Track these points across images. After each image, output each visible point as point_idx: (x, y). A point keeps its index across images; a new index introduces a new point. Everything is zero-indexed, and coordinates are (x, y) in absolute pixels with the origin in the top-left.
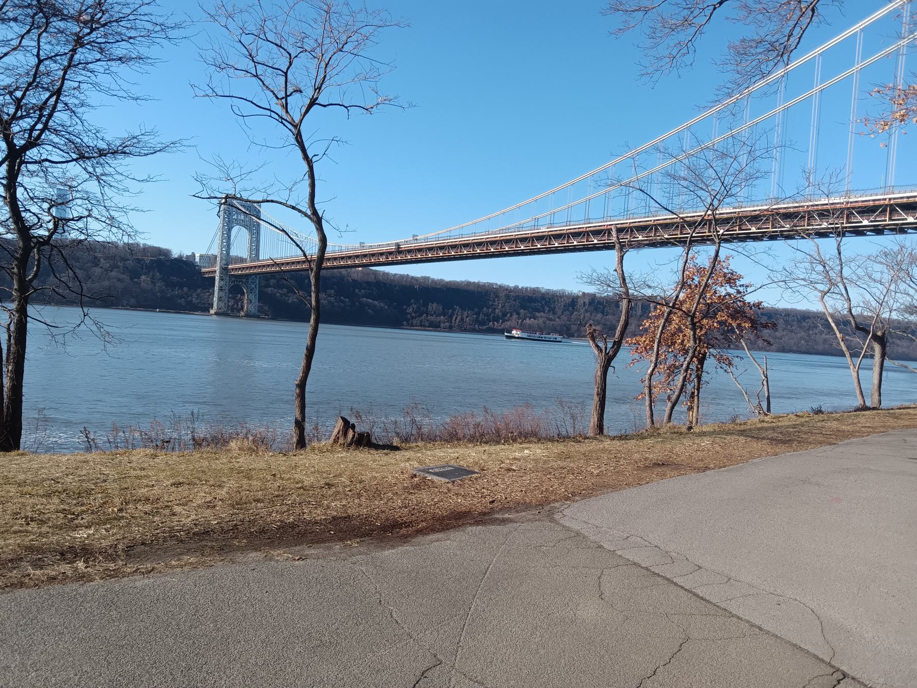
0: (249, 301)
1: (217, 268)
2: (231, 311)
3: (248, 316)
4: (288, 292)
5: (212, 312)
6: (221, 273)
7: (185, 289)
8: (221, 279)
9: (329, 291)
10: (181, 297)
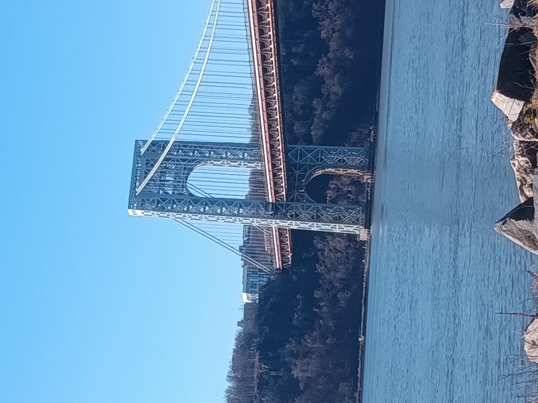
0: (341, 164)
1: (275, 224)
2: (362, 201)
3: (371, 167)
4: (320, 95)
5: (363, 235)
6: (284, 217)
7: (317, 294)
8: (296, 217)
9: (315, 14)
10: (335, 299)
